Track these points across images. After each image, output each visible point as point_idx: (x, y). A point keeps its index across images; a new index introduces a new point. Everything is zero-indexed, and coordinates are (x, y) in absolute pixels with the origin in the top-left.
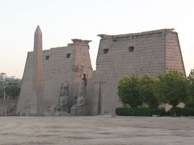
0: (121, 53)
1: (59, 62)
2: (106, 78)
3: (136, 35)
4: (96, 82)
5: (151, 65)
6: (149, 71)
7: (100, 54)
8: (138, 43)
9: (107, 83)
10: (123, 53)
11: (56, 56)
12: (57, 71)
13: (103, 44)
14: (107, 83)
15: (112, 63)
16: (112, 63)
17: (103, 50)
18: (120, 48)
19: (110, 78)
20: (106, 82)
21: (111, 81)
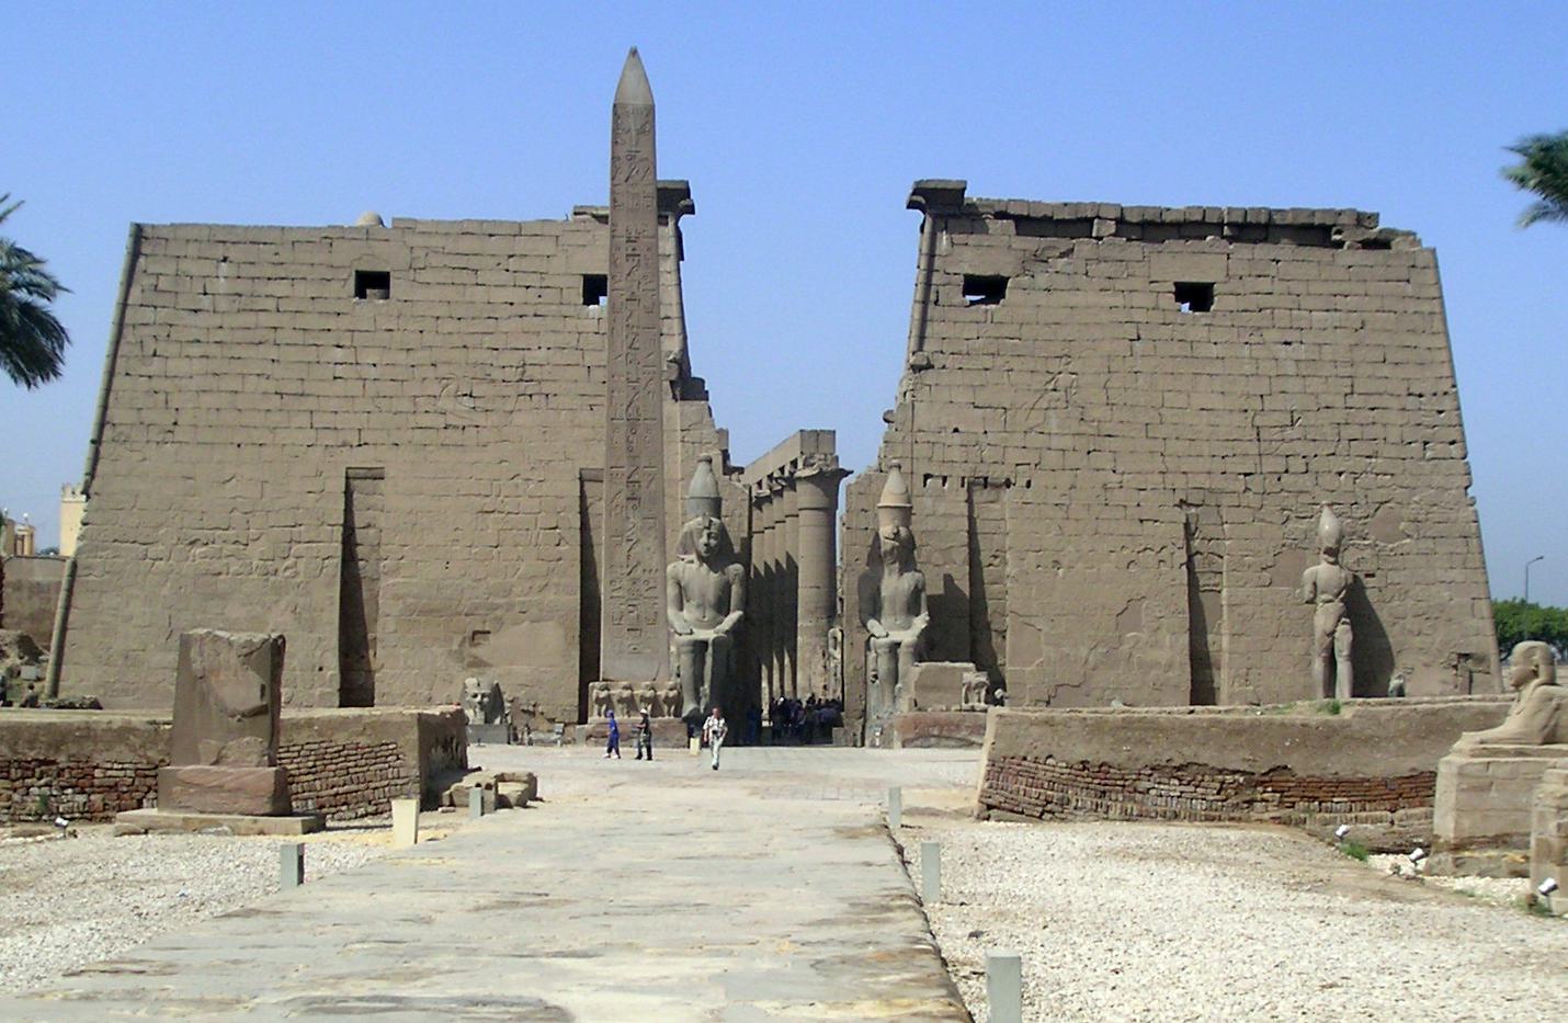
0: (1121, 316)
1: (504, 326)
2: (1014, 456)
3: (1148, 217)
4: (927, 477)
5: (1353, 401)
6: (1348, 432)
7: (936, 303)
8: (1238, 268)
9: (1028, 484)
10: (1139, 316)
12: (511, 390)
13: (953, 244)
14: (1028, 484)
15: (1055, 366)
16: (1055, 366)
17: (962, 278)
18: (1107, 284)
19: (1052, 459)
20: (1022, 482)
21: (1065, 479)
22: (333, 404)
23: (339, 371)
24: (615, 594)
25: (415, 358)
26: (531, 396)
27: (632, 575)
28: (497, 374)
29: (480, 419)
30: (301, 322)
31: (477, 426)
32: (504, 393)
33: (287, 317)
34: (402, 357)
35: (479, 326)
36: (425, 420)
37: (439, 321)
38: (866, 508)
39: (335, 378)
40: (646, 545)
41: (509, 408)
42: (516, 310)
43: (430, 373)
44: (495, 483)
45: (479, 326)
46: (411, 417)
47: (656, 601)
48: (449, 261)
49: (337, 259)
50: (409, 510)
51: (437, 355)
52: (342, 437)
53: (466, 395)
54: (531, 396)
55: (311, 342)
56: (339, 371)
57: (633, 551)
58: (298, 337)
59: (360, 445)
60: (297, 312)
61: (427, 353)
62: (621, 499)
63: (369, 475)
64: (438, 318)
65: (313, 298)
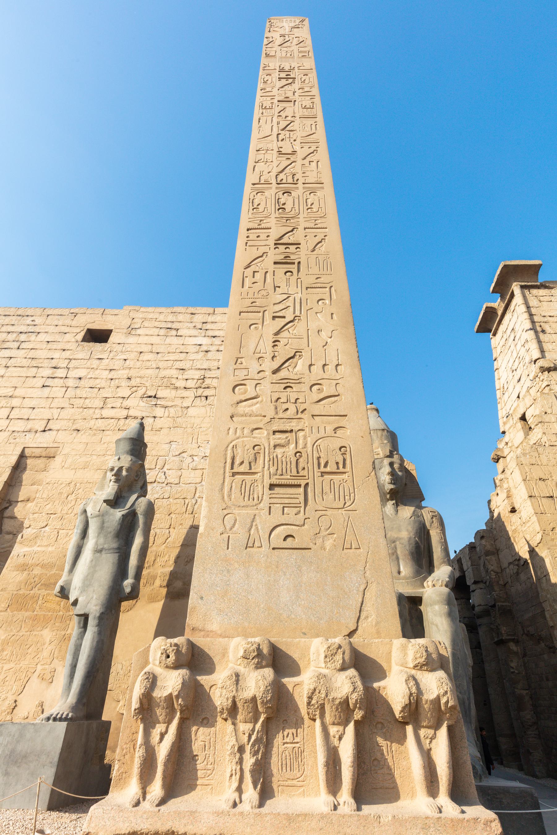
11: (174, 333)
22: (33, 403)
23: (49, 382)
24: (243, 408)
25: (113, 375)
26: (206, 397)
27: (283, 373)
28: (181, 384)
29: (159, 412)
30: (32, 354)
31: (155, 417)
32: (182, 396)
33: (24, 351)
34: (105, 374)
35: (172, 357)
36: (107, 413)
37: (142, 354)
38: (544, 477)
39: (43, 386)
40: (313, 326)
41: (185, 405)
42: (204, 348)
43: (124, 383)
44: (160, 458)
45: (172, 357)
46: (97, 411)
47: (343, 422)
48: (157, 324)
49: (74, 323)
50: (69, 481)
51: (132, 373)
52: (30, 425)
53: (150, 397)
54: (206, 397)
55: (35, 365)
56: (49, 382)
57: (284, 334)
58: (25, 363)
59: (44, 431)
60: (31, 349)
61: (127, 371)
62: (268, 263)
63: (44, 454)
64: (141, 352)
65: (48, 342)
